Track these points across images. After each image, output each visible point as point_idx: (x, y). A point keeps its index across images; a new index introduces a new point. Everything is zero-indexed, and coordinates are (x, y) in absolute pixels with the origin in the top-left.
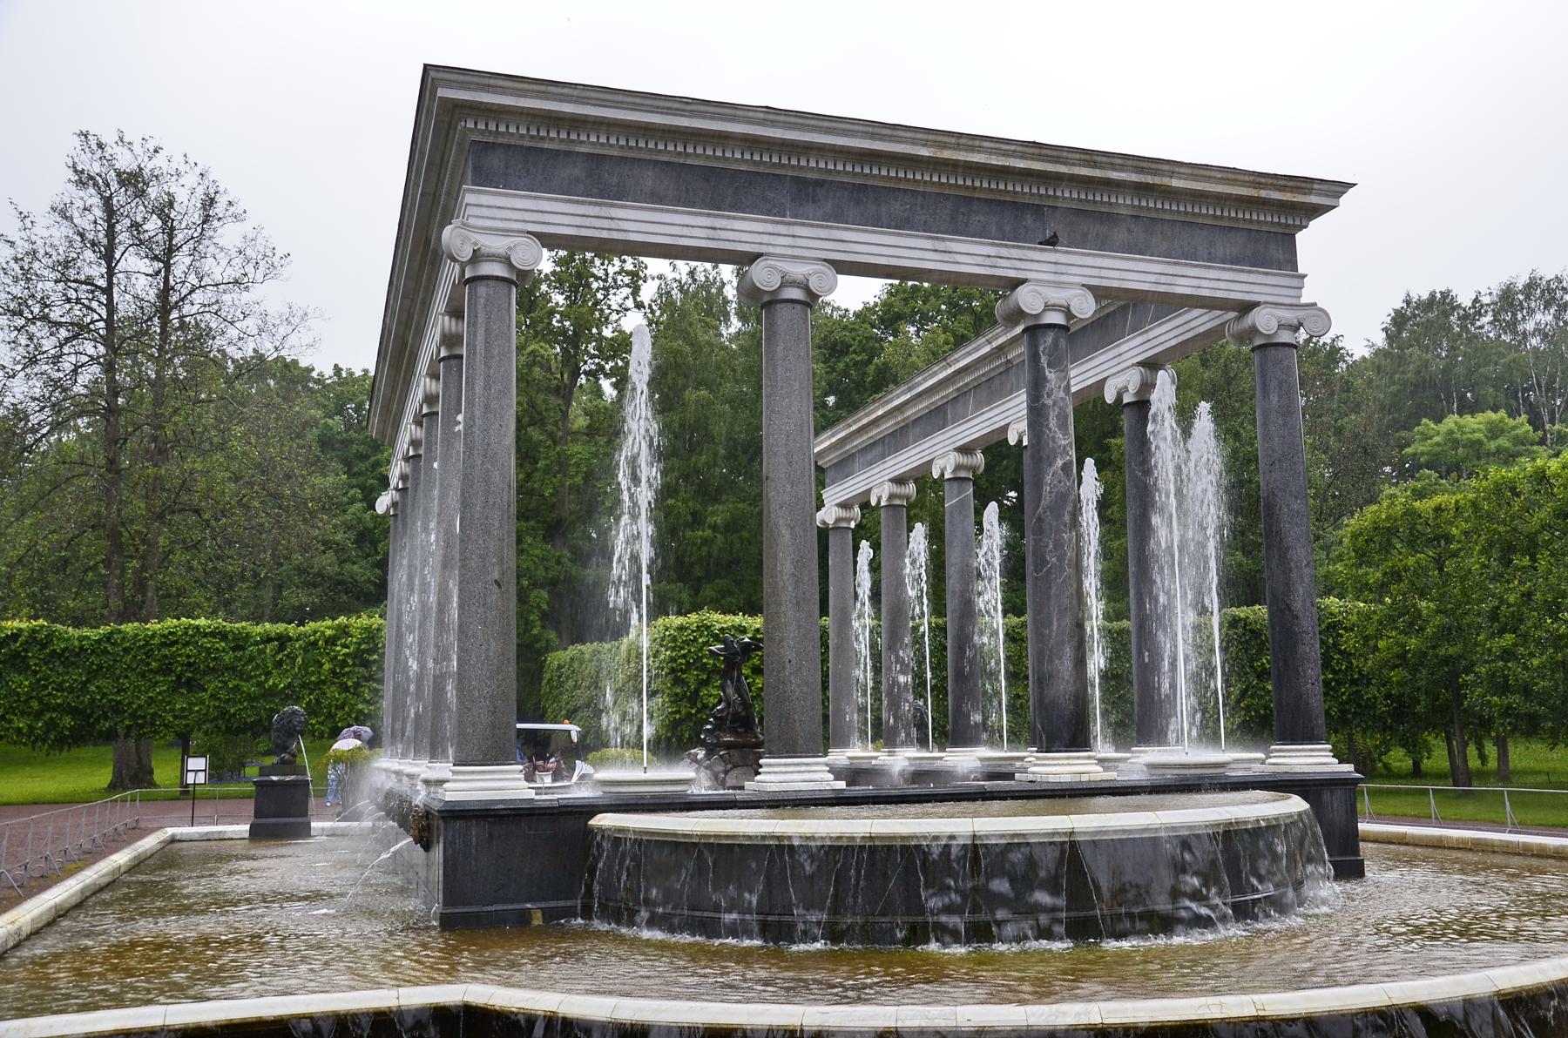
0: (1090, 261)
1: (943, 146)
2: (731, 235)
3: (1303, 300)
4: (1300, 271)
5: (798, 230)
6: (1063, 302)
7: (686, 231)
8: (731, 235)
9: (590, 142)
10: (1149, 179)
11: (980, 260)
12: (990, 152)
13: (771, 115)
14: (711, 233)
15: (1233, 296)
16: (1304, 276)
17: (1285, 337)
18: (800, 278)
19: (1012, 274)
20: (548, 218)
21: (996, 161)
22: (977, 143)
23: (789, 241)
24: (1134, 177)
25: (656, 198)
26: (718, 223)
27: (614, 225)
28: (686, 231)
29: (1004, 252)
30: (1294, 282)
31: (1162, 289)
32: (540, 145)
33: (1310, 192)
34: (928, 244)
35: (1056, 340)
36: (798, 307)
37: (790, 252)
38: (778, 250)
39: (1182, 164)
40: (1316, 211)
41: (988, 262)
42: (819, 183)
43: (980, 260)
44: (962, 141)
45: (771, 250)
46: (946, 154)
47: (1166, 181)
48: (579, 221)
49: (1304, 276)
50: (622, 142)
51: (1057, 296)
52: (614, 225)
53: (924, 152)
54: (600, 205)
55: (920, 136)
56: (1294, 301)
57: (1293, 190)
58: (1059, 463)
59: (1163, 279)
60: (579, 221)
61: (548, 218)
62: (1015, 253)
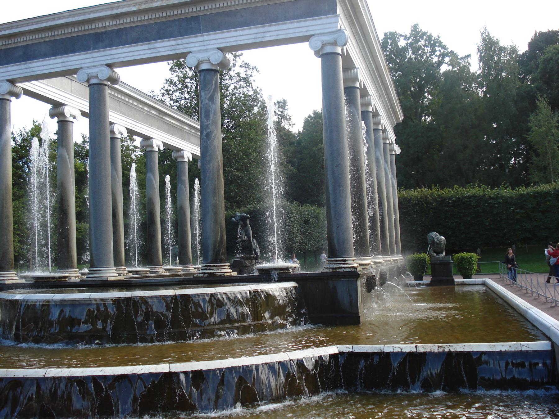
0: (220, 36)
2: (70, 63)
6: (206, 58)
8: (70, 63)
9: (22, 41)
11: (169, 48)
13: (71, 12)
17: (328, 49)
18: (94, 75)
23: (92, 60)
25: (45, 56)
26: (66, 59)
27: (31, 70)
29: (179, 42)
30: (333, 20)
35: (205, 77)
36: (95, 86)
37: (92, 64)
38: (85, 65)
41: (173, 48)
42: (103, 33)
43: (169, 48)
46: (144, 7)
51: (202, 56)
52: (31, 70)
53: (134, 9)
56: (334, 30)
59: (258, 36)
62: (184, 41)
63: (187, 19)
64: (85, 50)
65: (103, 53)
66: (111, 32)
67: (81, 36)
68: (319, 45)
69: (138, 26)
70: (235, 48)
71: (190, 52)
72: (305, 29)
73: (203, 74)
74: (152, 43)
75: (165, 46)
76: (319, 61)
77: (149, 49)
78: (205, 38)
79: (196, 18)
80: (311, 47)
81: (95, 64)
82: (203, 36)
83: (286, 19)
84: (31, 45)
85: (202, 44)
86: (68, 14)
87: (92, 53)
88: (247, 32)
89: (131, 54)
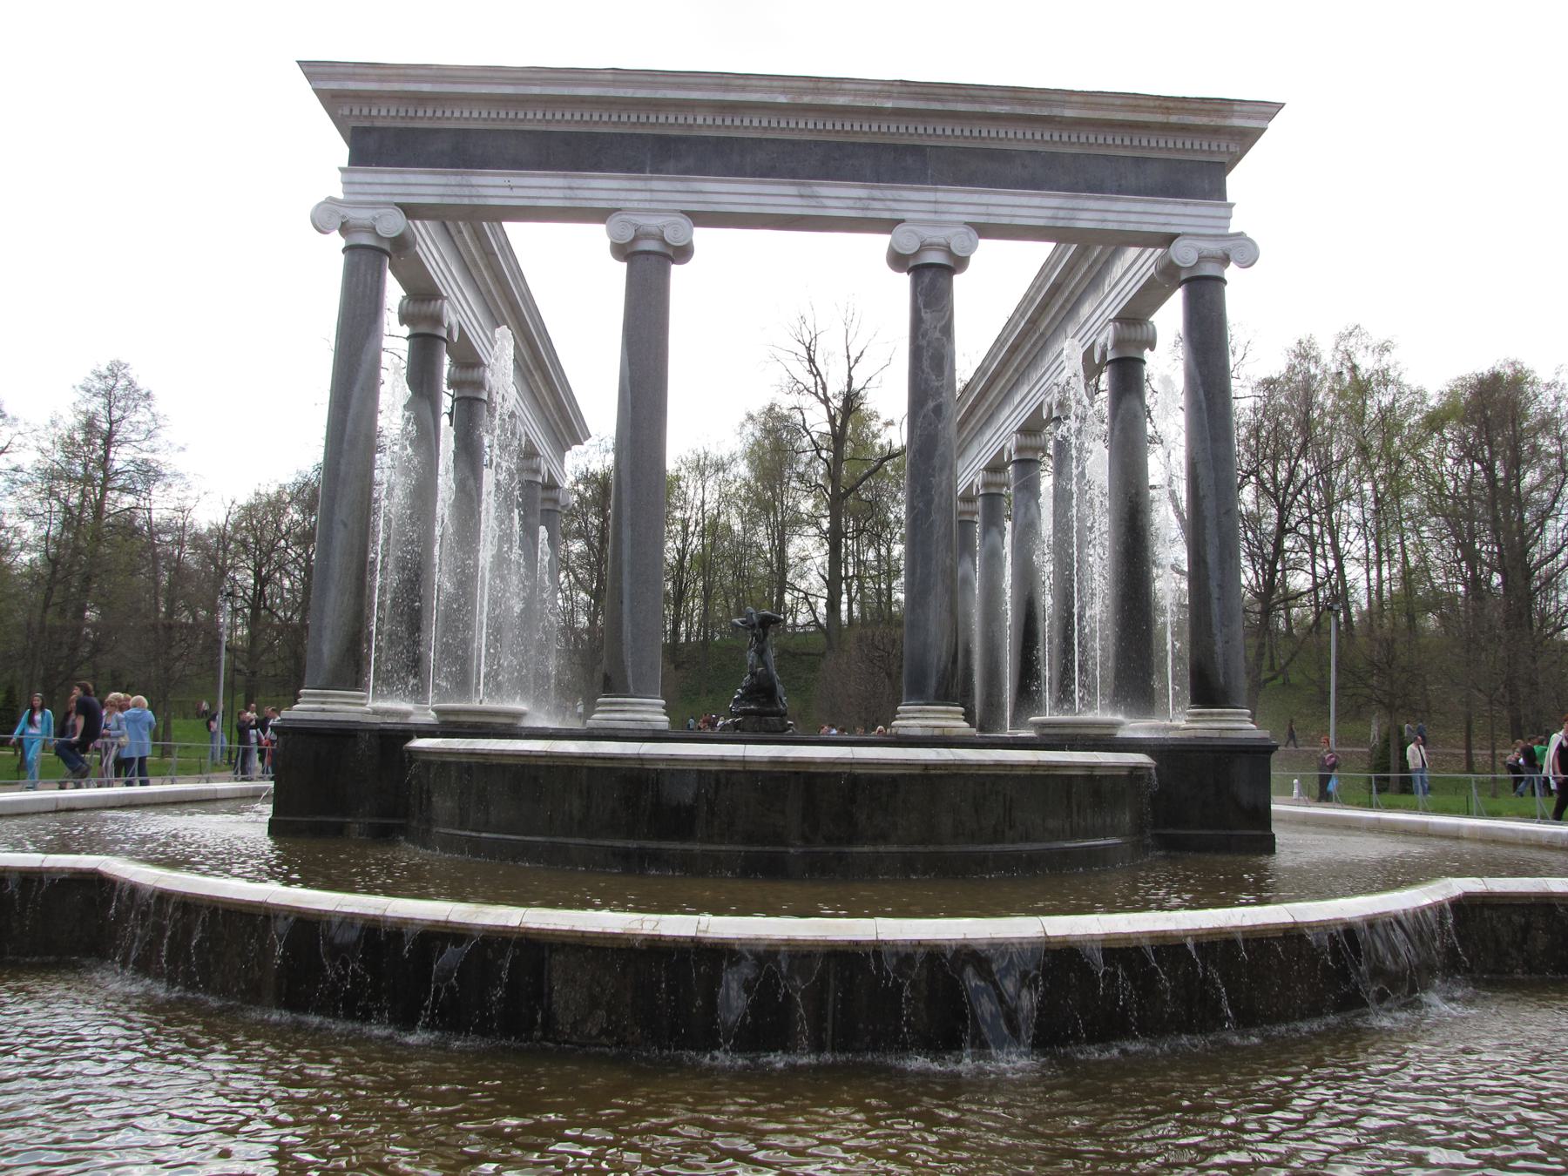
0: (975, 198)
1: (804, 91)
2: (587, 194)
3: (1232, 230)
4: (1230, 200)
5: (656, 185)
6: (942, 241)
7: (543, 193)
8: (587, 194)
10: (1036, 111)
11: (850, 203)
12: (856, 93)
14: (569, 193)
15: (1145, 228)
16: (1231, 205)
18: (654, 230)
19: (886, 215)
20: (413, 190)
21: (859, 102)
22: (837, 86)
23: (647, 196)
24: (1019, 110)
28: (543, 193)
29: (876, 193)
30: (1222, 212)
31: (1060, 224)
32: (411, 125)
33: (1232, 114)
34: (792, 190)
36: (653, 258)
37: (647, 206)
39: (1072, 93)
40: (1248, 137)
41: (859, 204)
43: (850, 203)
44: (821, 85)
45: (628, 205)
46: (807, 99)
47: (1056, 112)
48: (441, 190)
49: (1231, 205)
50: (615, 118)
52: (474, 191)
53: (782, 99)
54: (461, 174)
55: (775, 83)
56: (1221, 232)
57: (1208, 113)
58: (931, 404)
59: (1061, 214)
60: (441, 190)
61: (413, 190)
62: (889, 194)
63: (895, 148)
64: (629, 170)
65: (679, 186)
66: (705, 140)
67: (622, 135)
68: (629, 235)
69: (774, 141)
70: (987, 230)
71: (903, 221)
72: (1162, 219)
73: (927, 277)
74: (810, 185)
75: (600, 187)
76: (622, 267)
77: (801, 196)
78: (940, 196)
79: (917, 150)
80: (610, 234)
81: (654, 205)
82: (936, 190)
83: (1121, 190)
84: (477, 131)
85: (930, 207)
86: (610, 77)
87: (651, 179)
88: (1036, 201)
89: (753, 199)
